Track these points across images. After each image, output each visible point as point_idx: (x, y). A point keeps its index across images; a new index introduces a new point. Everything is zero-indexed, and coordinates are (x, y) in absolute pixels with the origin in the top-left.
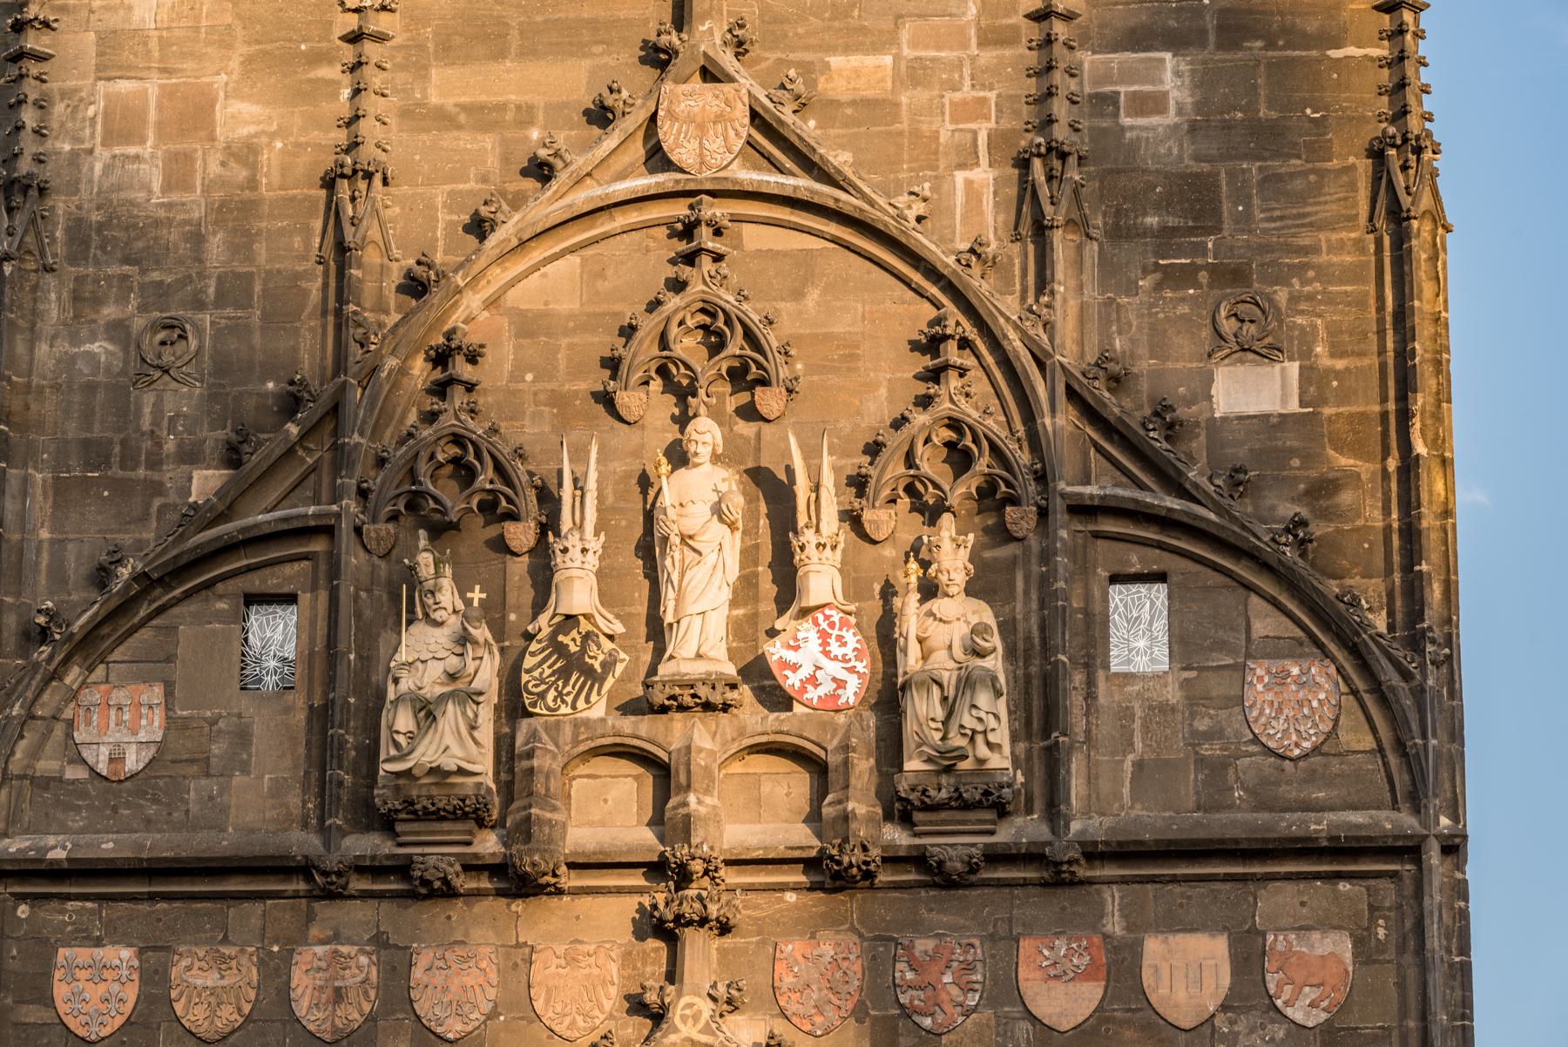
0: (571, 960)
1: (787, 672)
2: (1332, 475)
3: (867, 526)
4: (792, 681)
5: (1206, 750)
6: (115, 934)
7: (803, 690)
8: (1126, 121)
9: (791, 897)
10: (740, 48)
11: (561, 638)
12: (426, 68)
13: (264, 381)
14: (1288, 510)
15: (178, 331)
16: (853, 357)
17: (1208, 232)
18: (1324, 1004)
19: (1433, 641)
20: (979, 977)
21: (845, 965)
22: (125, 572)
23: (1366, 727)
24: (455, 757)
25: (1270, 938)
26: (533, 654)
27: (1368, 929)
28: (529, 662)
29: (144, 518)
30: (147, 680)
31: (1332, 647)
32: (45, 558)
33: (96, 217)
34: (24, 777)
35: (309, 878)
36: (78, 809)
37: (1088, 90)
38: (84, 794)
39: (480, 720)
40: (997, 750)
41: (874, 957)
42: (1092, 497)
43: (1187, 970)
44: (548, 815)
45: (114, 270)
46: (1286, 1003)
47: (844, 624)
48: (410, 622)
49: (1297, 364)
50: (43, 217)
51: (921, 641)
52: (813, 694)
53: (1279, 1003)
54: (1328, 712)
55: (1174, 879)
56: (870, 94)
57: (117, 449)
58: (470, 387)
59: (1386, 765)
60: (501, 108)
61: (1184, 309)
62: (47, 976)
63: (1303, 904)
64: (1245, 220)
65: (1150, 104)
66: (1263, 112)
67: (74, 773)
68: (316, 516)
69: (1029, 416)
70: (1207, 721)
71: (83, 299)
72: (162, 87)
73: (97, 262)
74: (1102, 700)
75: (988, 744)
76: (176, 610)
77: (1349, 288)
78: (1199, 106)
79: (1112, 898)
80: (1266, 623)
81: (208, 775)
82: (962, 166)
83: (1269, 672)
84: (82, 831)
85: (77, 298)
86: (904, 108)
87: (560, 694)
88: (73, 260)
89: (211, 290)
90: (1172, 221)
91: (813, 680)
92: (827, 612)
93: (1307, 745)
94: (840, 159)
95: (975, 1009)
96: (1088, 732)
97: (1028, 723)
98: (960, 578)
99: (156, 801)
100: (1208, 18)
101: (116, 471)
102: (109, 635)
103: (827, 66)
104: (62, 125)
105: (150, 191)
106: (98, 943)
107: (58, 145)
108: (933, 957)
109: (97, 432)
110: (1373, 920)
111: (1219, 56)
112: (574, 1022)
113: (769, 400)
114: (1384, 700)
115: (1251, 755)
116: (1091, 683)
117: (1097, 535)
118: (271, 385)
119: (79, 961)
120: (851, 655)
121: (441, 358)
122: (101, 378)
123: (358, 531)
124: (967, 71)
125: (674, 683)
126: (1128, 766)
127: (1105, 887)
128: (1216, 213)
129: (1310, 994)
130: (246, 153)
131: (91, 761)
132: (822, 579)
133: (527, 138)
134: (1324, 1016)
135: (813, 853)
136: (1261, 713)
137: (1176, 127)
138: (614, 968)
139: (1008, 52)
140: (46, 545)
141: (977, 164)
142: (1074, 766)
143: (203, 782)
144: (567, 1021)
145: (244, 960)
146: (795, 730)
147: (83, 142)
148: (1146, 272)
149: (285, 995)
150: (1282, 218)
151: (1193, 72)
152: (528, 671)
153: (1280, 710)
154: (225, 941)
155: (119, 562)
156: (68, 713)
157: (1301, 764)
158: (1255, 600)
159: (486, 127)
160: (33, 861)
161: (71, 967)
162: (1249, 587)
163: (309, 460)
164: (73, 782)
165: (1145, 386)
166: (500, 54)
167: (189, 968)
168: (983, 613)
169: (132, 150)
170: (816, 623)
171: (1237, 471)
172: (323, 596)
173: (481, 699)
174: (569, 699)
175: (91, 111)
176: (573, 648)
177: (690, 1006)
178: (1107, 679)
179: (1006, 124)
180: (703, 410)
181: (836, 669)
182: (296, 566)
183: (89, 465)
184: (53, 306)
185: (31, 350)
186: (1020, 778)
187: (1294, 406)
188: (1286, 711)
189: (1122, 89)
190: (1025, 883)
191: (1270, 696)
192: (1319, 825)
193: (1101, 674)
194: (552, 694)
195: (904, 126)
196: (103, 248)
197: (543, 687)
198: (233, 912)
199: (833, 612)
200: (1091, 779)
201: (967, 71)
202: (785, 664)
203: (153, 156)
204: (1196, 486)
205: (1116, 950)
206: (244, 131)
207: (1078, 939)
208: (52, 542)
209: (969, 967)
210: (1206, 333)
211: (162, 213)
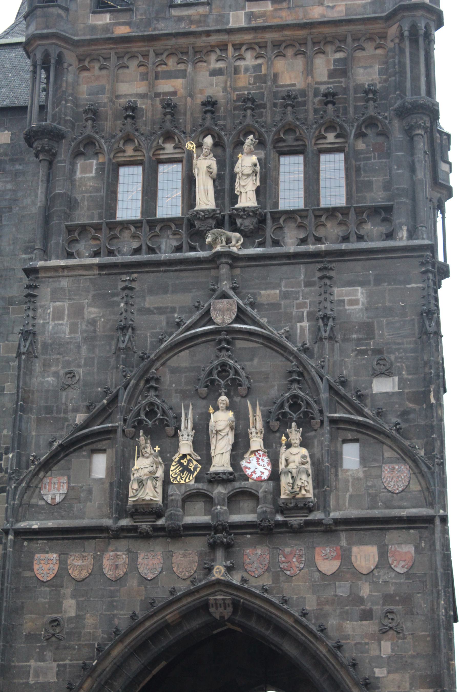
0: (185, 556)
1: (247, 470)
2: (407, 410)
4: (248, 472)
5: (371, 491)
6: (52, 550)
7: (252, 475)
8: (347, 307)
9: (249, 536)
10: (234, 289)
11: (182, 461)
12: (144, 297)
13: (98, 388)
14: (394, 420)
15: (72, 374)
16: (267, 378)
17: (371, 339)
18: (406, 566)
19: (437, 458)
20: (303, 559)
21: (264, 556)
22: (56, 444)
23: (418, 484)
25: (390, 547)
26: (173, 466)
27: (419, 544)
28: (172, 468)
29: (62, 428)
30: (63, 475)
31: (408, 460)
32: (34, 440)
33: (50, 341)
34: (27, 504)
35: (108, 533)
36: (42, 513)
37: (336, 298)
38: (44, 509)
39: (157, 485)
40: (308, 491)
41: (273, 554)
42: (336, 417)
43: (365, 556)
44: (177, 513)
45: (55, 357)
46: (395, 566)
47: (263, 455)
48: (138, 457)
49: (397, 377)
50: (34, 342)
51: (287, 460)
52: (254, 476)
53: (392, 566)
54: (407, 480)
55: (361, 530)
56: (272, 301)
57: (55, 408)
58: (156, 389)
59: (424, 495)
60: (166, 308)
61: (364, 362)
62: (32, 563)
63: (399, 536)
64: (382, 336)
65: (354, 302)
66: (388, 304)
67: (41, 503)
68: (111, 427)
69: (318, 394)
70: (371, 482)
71: (46, 365)
72: (69, 304)
73: (50, 355)
74: (340, 477)
75: (305, 490)
76: (71, 455)
77: (412, 355)
78: (368, 303)
79: (343, 536)
80: (388, 454)
81: (80, 503)
82: (300, 322)
83: (389, 468)
84: (43, 520)
85: (44, 365)
86: (282, 305)
87: (181, 478)
88: (43, 354)
89: (83, 362)
90: (360, 336)
91: (254, 472)
93: (400, 489)
94: (264, 321)
95: (302, 569)
96: (336, 486)
97: (318, 483)
98: (298, 442)
99: (65, 511)
100: (371, 277)
101: (55, 415)
102: (52, 462)
103: (260, 293)
104: (40, 315)
105: (65, 334)
106: (47, 553)
107: (39, 321)
108: (291, 553)
109: (49, 404)
110: (420, 541)
111: (374, 288)
112: (185, 574)
113: (242, 390)
114: (423, 476)
115: (384, 492)
116: (337, 471)
117: (338, 429)
118: (99, 389)
119: (42, 558)
120: (266, 465)
121: (147, 381)
122: (51, 388)
123: (124, 431)
124: (301, 294)
126: (348, 496)
127: (341, 532)
128: (373, 333)
129: (402, 563)
130: (93, 322)
131: (46, 499)
132: (256, 443)
133: (174, 317)
134: (406, 570)
135: (255, 523)
136: (387, 479)
137: (361, 309)
138: (197, 558)
139: (313, 288)
140: (34, 437)
141: (304, 321)
142: (331, 497)
143: (79, 505)
144: (183, 573)
145: (89, 557)
146: (249, 487)
147: (46, 320)
148: (353, 351)
149: (101, 568)
150: (393, 334)
151: (367, 293)
153: (392, 479)
154: (84, 551)
155: (55, 441)
156: (40, 486)
157: (399, 495)
158: (385, 447)
159: (161, 314)
160: (28, 529)
161: (40, 560)
162: (383, 443)
163: (110, 411)
164: (41, 506)
165: (352, 385)
166: (166, 292)
167: (73, 560)
168: (304, 451)
169: (60, 322)
170: (255, 455)
171: (379, 409)
172: (114, 450)
174: (184, 479)
175: (49, 311)
176: (185, 464)
177: (218, 568)
178: (342, 470)
179: (312, 309)
180: (223, 394)
182: (106, 442)
183: (47, 413)
184: (37, 366)
185: (30, 380)
186: (316, 500)
187: (396, 390)
188: (394, 479)
189: (346, 298)
190: (317, 531)
191: (389, 475)
192: (404, 513)
193: (339, 469)
195: (282, 310)
196: (52, 350)
198: (86, 543)
199: (260, 452)
200: (337, 499)
201: (301, 294)
202: (246, 468)
203: (66, 324)
204: (367, 413)
205: (344, 551)
206: (93, 316)
207: (333, 548)
208: (36, 435)
209: (301, 556)
210: (370, 369)
211: (69, 340)
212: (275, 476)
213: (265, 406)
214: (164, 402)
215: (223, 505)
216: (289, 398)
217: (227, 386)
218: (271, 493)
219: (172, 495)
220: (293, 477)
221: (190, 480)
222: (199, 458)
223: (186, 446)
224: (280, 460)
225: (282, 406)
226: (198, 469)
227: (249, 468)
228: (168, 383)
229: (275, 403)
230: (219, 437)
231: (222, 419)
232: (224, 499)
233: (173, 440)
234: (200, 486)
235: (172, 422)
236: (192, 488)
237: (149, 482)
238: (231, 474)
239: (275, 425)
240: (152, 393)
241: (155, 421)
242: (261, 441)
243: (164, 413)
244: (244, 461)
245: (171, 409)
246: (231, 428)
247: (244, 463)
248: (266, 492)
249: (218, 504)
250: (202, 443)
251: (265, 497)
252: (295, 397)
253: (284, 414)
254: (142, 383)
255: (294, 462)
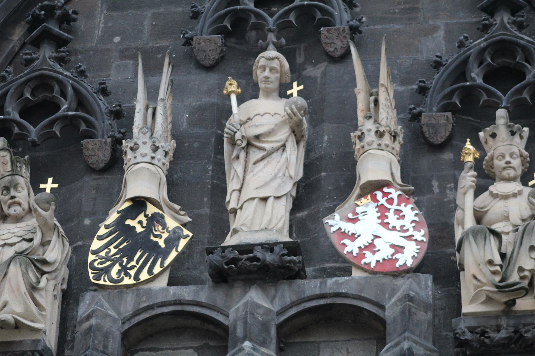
1: (346, 241)
3: (425, 129)
4: (351, 247)
7: (361, 255)
11: (129, 222)
24: (12, 312)
26: (100, 238)
28: (96, 244)
39: (43, 284)
52: (370, 259)
87: (125, 270)
91: (371, 247)
92: (386, 190)
113: (332, 40)
120: (409, 226)
125: (234, 247)
132: (378, 162)
146: (352, 291)
152: (95, 252)
173: (46, 269)
174: (132, 272)
176: (139, 229)
180: (271, 46)
181: (396, 238)
194: (117, 267)
197: (109, 263)
199: (391, 190)
202: (342, 234)
212: (441, 263)
213: (404, 82)
214: (82, 73)
215: (264, 343)
216: (483, 50)
217: (283, 27)
218: (426, 307)
219: (88, 317)
220: (503, 256)
221: (152, 280)
222: (187, 219)
223: (144, 179)
224: (458, 213)
225: (461, 72)
226: (183, 243)
227: (353, 237)
228: (98, 32)
229: (437, 65)
230: (255, 155)
231: (264, 114)
232: (265, 326)
233: (108, 177)
234: (186, 293)
235: (104, 124)
236: (160, 300)
237: (15, 270)
238: (292, 248)
239: (439, 122)
240: (47, 52)
241: (51, 124)
242: (395, 160)
243: (81, 102)
244: (337, 216)
245: (104, 92)
246: (296, 132)
247: (335, 222)
248: (411, 299)
249: (245, 339)
250: (200, 170)
251: (407, 315)
252: (503, 48)
253: (469, 95)
254: (17, 34)
255: (506, 218)
